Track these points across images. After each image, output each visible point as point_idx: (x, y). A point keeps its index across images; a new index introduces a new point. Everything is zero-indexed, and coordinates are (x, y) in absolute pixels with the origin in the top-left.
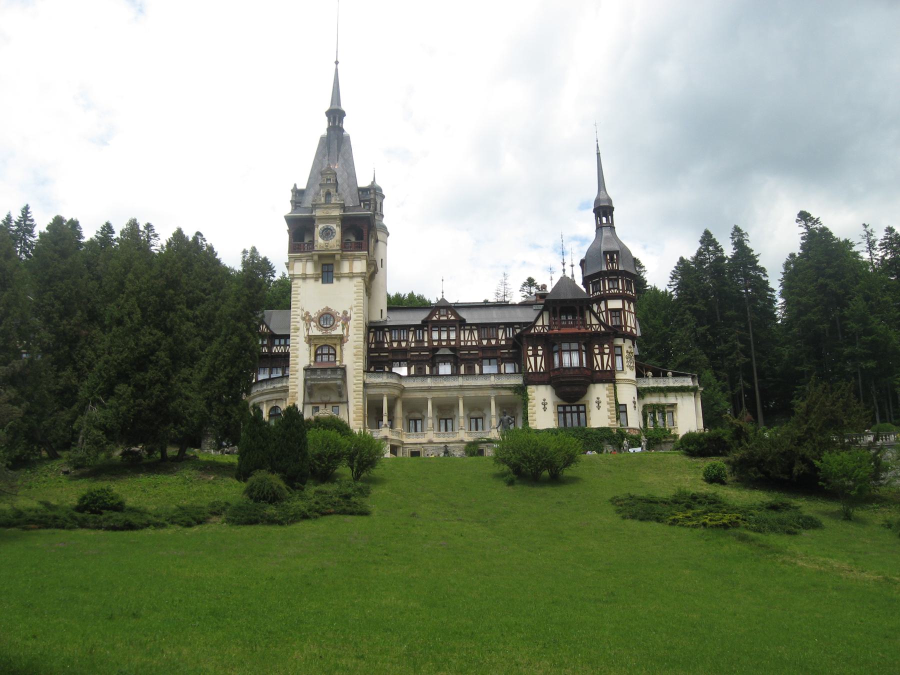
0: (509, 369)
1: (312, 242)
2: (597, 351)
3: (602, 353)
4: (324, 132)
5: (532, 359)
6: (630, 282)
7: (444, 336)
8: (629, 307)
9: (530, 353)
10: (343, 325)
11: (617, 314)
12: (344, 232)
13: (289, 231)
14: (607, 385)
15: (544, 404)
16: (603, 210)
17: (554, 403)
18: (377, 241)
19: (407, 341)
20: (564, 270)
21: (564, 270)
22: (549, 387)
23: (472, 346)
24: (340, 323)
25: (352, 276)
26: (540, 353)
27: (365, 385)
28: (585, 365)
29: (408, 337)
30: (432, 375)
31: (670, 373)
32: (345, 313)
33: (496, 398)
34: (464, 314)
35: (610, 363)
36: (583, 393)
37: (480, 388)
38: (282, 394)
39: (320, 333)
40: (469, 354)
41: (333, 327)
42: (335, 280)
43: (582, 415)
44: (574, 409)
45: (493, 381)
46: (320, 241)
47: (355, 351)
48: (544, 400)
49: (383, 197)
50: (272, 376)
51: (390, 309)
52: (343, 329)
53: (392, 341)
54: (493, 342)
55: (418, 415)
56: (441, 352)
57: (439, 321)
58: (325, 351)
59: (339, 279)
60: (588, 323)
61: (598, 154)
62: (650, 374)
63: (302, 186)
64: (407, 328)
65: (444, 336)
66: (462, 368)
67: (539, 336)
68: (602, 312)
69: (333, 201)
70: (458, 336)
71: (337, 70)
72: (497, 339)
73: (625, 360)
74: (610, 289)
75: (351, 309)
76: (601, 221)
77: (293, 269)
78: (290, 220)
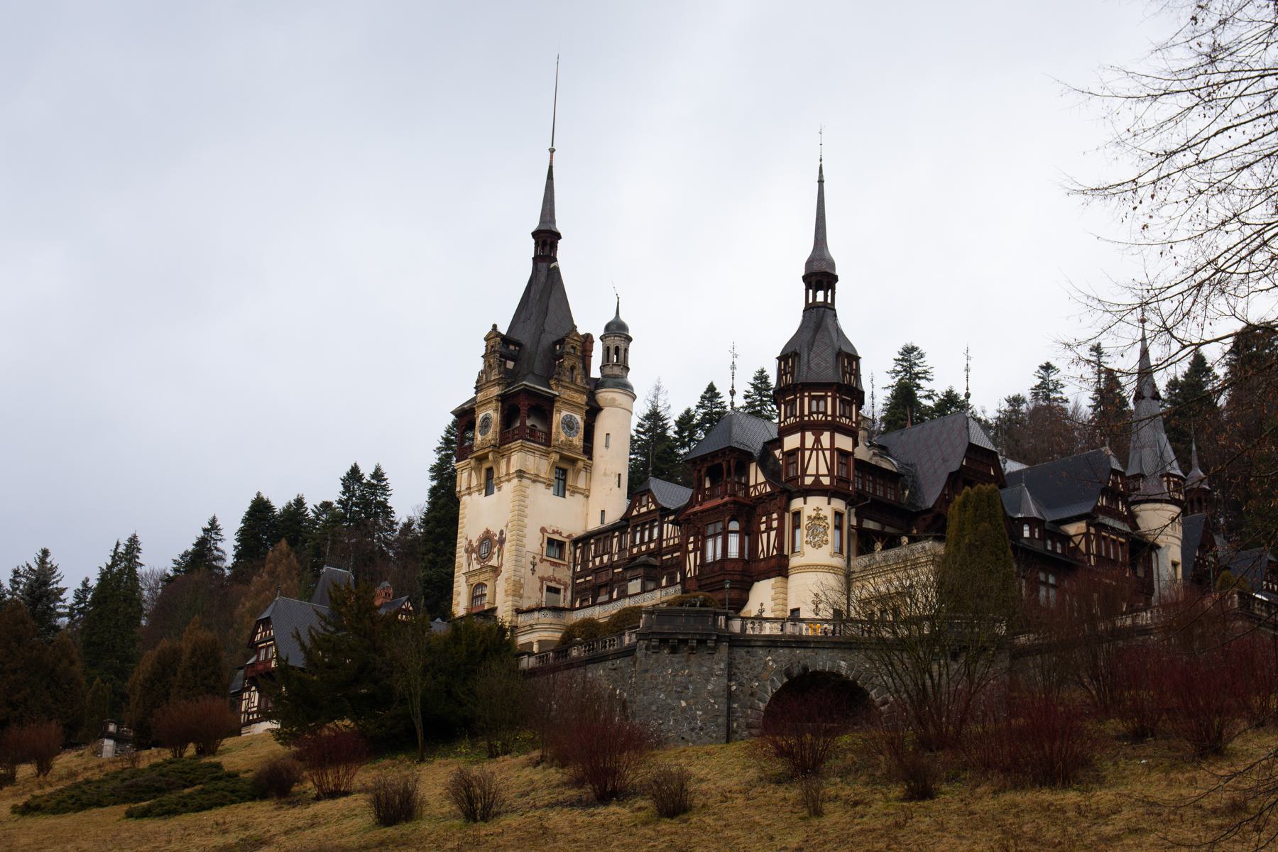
2: (763, 527)
3: (769, 529)
6: (824, 398)
8: (817, 441)
9: (691, 547)
12: (509, 416)
16: (820, 277)
19: (611, 554)
31: (905, 539)
41: (489, 557)
46: (479, 437)
57: (639, 515)
61: (821, 182)
62: (878, 546)
66: (664, 582)
76: (815, 297)
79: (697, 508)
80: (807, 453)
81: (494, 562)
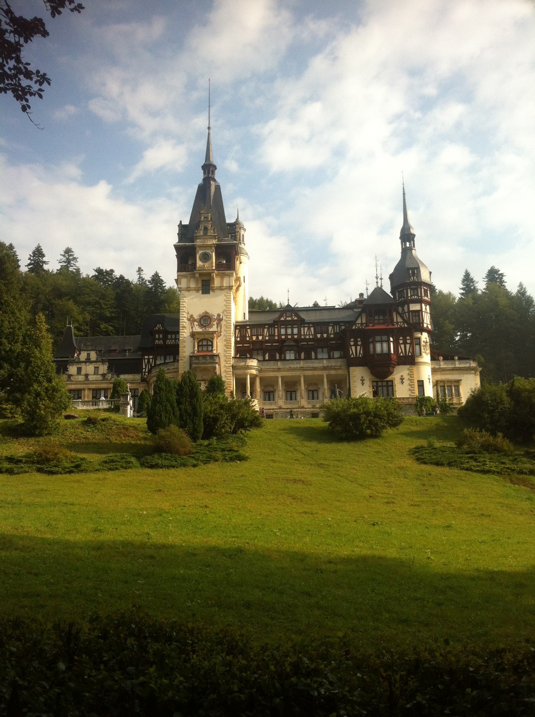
0: (337, 354)
1: (195, 264)
2: (401, 342)
3: (405, 343)
4: (200, 181)
5: (353, 348)
7: (289, 331)
8: (426, 309)
9: (352, 343)
10: (218, 324)
11: (417, 314)
13: (177, 256)
14: (408, 366)
15: (363, 380)
16: (407, 236)
17: (370, 380)
18: (241, 263)
19: (263, 335)
20: (377, 283)
21: (377, 283)
22: (366, 367)
23: (309, 338)
24: (215, 323)
25: (221, 288)
26: (359, 343)
27: (234, 367)
28: (392, 352)
29: (263, 331)
30: (280, 359)
31: (456, 358)
32: (219, 315)
33: (327, 375)
34: (303, 315)
35: (411, 351)
36: (391, 373)
37: (315, 369)
38: (175, 374)
39: (200, 330)
40: (308, 344)
41: (210, 325)
42: (211, 292)
43: (390, 388)
44: (385, 384)
45: (325, 363)
46: (199, 263)
47: (225, 343)
48: (362, 377)
49: (245, 230)
50: (167, 361)
51: (249, 312)
52: (217, 327)
53: (252, 335)
54: (325, 336)
55: (271, 389)
56: (287, 344)
57: (285, 321)
58: (205, 343)
59: (213, 290)
60: (395, 321)
61: (404, 194)
63: (186, 221)
64: (262, 326)
65: (289, 331)
66: (303, 355)
67: (359, 330)
68: (405, 313)
69: (209, 234)
70: (299, 331)
71: (209, 134)
72: (327, 332)
73: (422, 348)
74: (411, 296)
75: (223, 312)
76: (405, 245)
77: (180, 284)
78: (177, 247)
79: (370, 328)
80: (424, 313)
81: (214, 329)
